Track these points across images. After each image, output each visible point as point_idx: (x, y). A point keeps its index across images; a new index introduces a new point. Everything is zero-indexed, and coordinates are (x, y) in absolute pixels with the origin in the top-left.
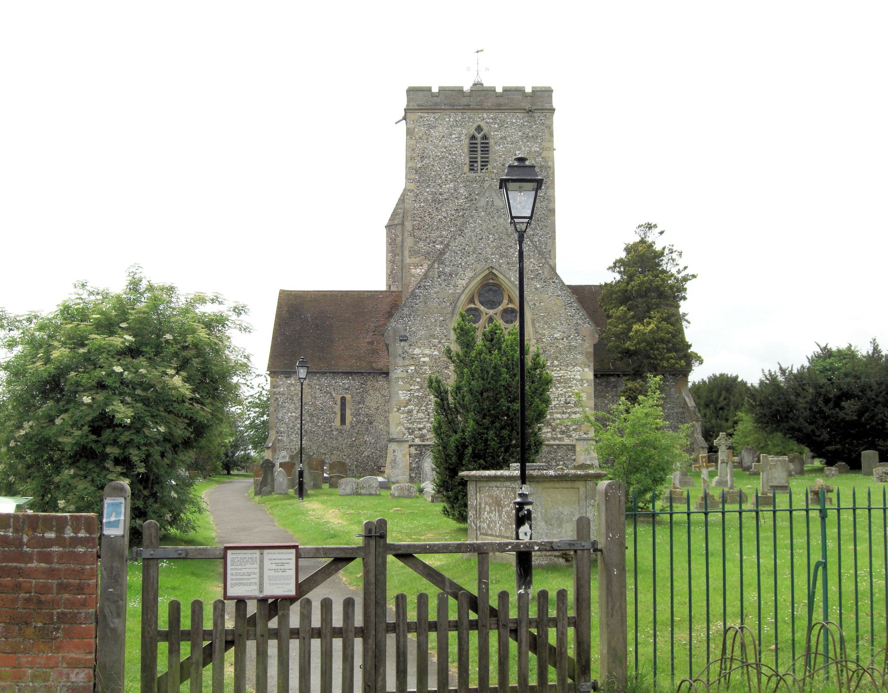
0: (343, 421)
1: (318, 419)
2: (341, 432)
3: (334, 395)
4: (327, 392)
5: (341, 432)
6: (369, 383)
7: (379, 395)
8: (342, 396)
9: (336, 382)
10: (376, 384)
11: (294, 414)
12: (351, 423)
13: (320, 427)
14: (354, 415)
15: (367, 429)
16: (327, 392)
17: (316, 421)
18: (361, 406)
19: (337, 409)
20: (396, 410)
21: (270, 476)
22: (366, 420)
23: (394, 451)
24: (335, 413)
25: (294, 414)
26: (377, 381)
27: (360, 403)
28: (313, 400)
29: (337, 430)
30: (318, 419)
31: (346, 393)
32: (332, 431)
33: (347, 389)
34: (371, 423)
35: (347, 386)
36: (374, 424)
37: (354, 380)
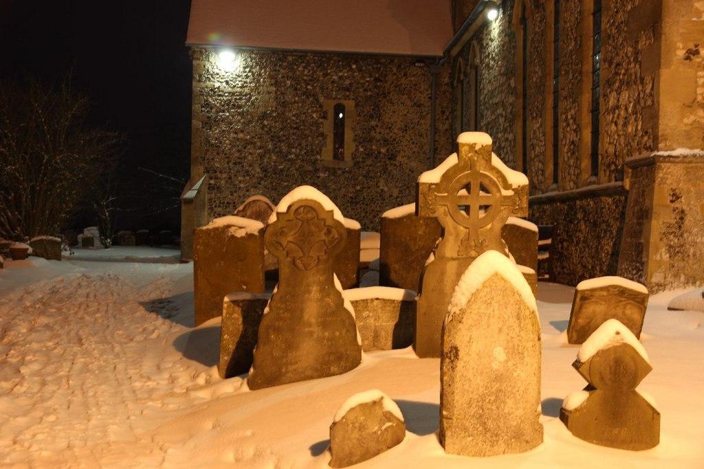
0: (338, 156)
1: (290, 146)
2: (334, 174)
3: (322, 99)
4: (307, 94)
5: (334, 174)
6: (390, 78)
7: (408, 103)
8: (335, 102)
9: (326, 75)
10: (403, 80)
11: (241, 135)
12: (354, 156)
13: (292, 161)
14: (359, 141)
15: (385, 169)
16: (307, 94)
17: (285, 149)
18: (373, 123)
19: (328, 127)
20: (681, 53)
21: (315, 292)
22: (383, 150)
23: (676, 197)
24: (322, 135)
25: (241, 135)
26: (405, 75)
27: (372, 117)
28: (280, 110)
29: (326, 169)
30: (290, 146)
31: (347, 97)
32: (317, 170)
33: (348, 90)
34: (392, 157)
35: (347, 82)
36: (399, 158)
37: (360, 70)
